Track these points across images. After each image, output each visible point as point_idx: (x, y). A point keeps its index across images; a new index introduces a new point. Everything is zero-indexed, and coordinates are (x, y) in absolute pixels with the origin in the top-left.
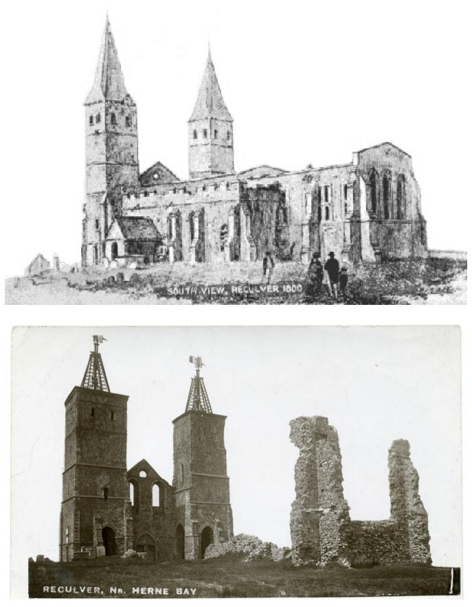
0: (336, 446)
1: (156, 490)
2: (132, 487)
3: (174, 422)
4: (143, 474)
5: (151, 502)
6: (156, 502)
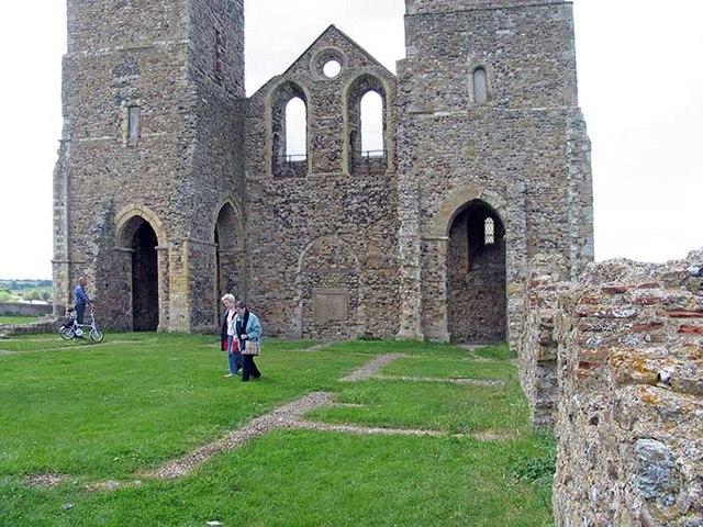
1: (371, 105)
4: (332, 69)
6: (372, 141)
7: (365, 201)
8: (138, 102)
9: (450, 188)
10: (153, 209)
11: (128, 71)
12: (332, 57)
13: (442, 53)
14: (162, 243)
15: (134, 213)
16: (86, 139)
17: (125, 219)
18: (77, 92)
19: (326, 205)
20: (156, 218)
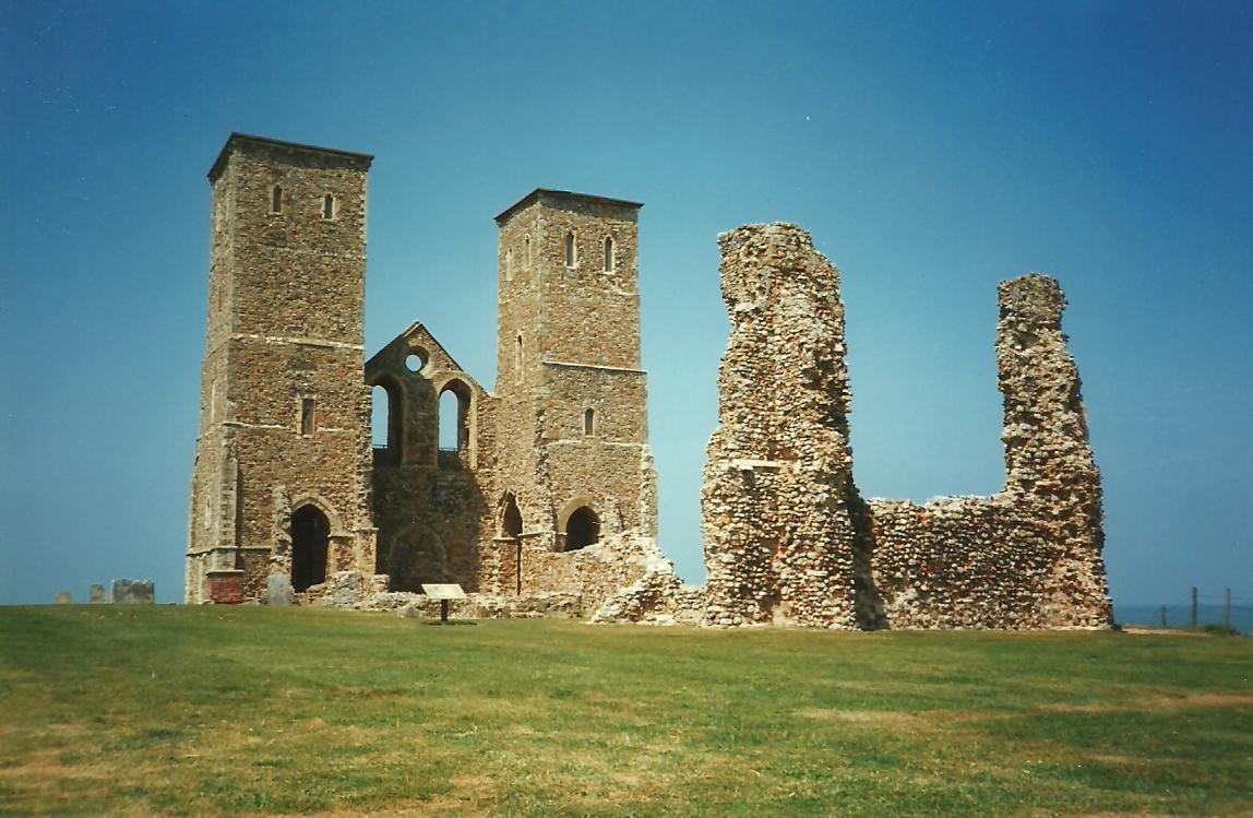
1: (448, 404)
3: (503, 219)
5: (434, 438)
6: (447, 439)
7: (452, 493)
10: (330, 499)
11: (303, 365)
13: (566, 396)
14: (337, 530)
15: (308, 502)
19: (417, 496)
20: (330, 507)
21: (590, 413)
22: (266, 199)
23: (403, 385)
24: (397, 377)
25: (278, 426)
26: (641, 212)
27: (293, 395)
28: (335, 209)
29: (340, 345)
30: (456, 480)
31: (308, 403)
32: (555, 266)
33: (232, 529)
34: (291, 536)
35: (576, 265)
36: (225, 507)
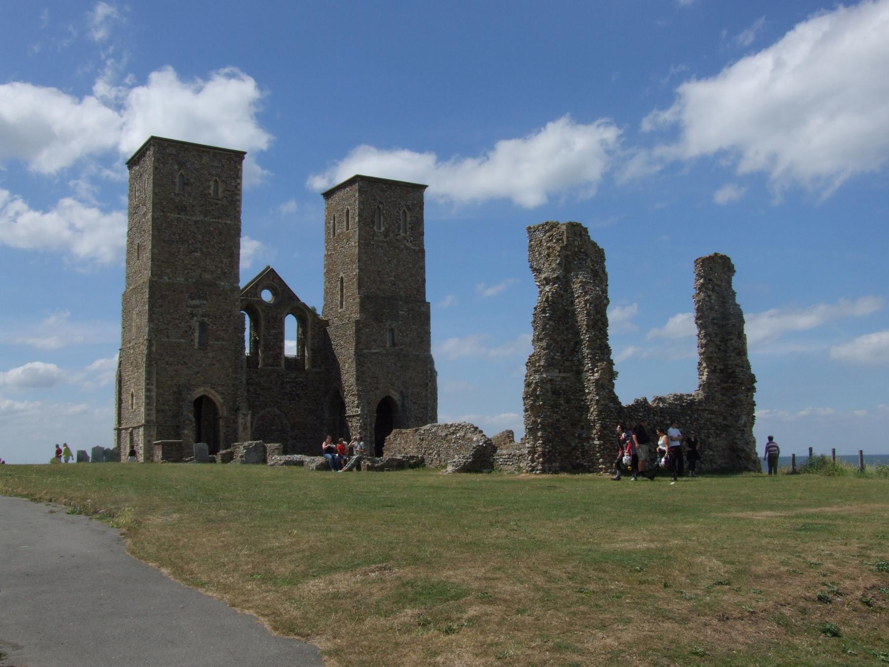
0: (600, 272)
1: (291, 324)
2: (247, 319)
3: (328, 195)
4: (267, 296)
5: (282, 348)
6: (291, 348)
8: (206, 319)
9: (378, 388)
11: (200, 298)
12: (268, 288)
14: (223, 412)
15: (202, 394)
16: (166, 340)
17: (198, 396)
18: (161, 306)
20: (219, 397)
21: (392, 330)
22: (173, 183)
23: (260, 311)
24: (258, 307)
25: (183, 340)
26: (427, 193)
27: (191, 319)
28: (220, 190)
29: (223, 283)
30: (296, 378)
31: (203, 325)
32: (368, 228)
33: (154, 412)
34: (194, 416)
35: (383, 229)
36: (148, 397)
